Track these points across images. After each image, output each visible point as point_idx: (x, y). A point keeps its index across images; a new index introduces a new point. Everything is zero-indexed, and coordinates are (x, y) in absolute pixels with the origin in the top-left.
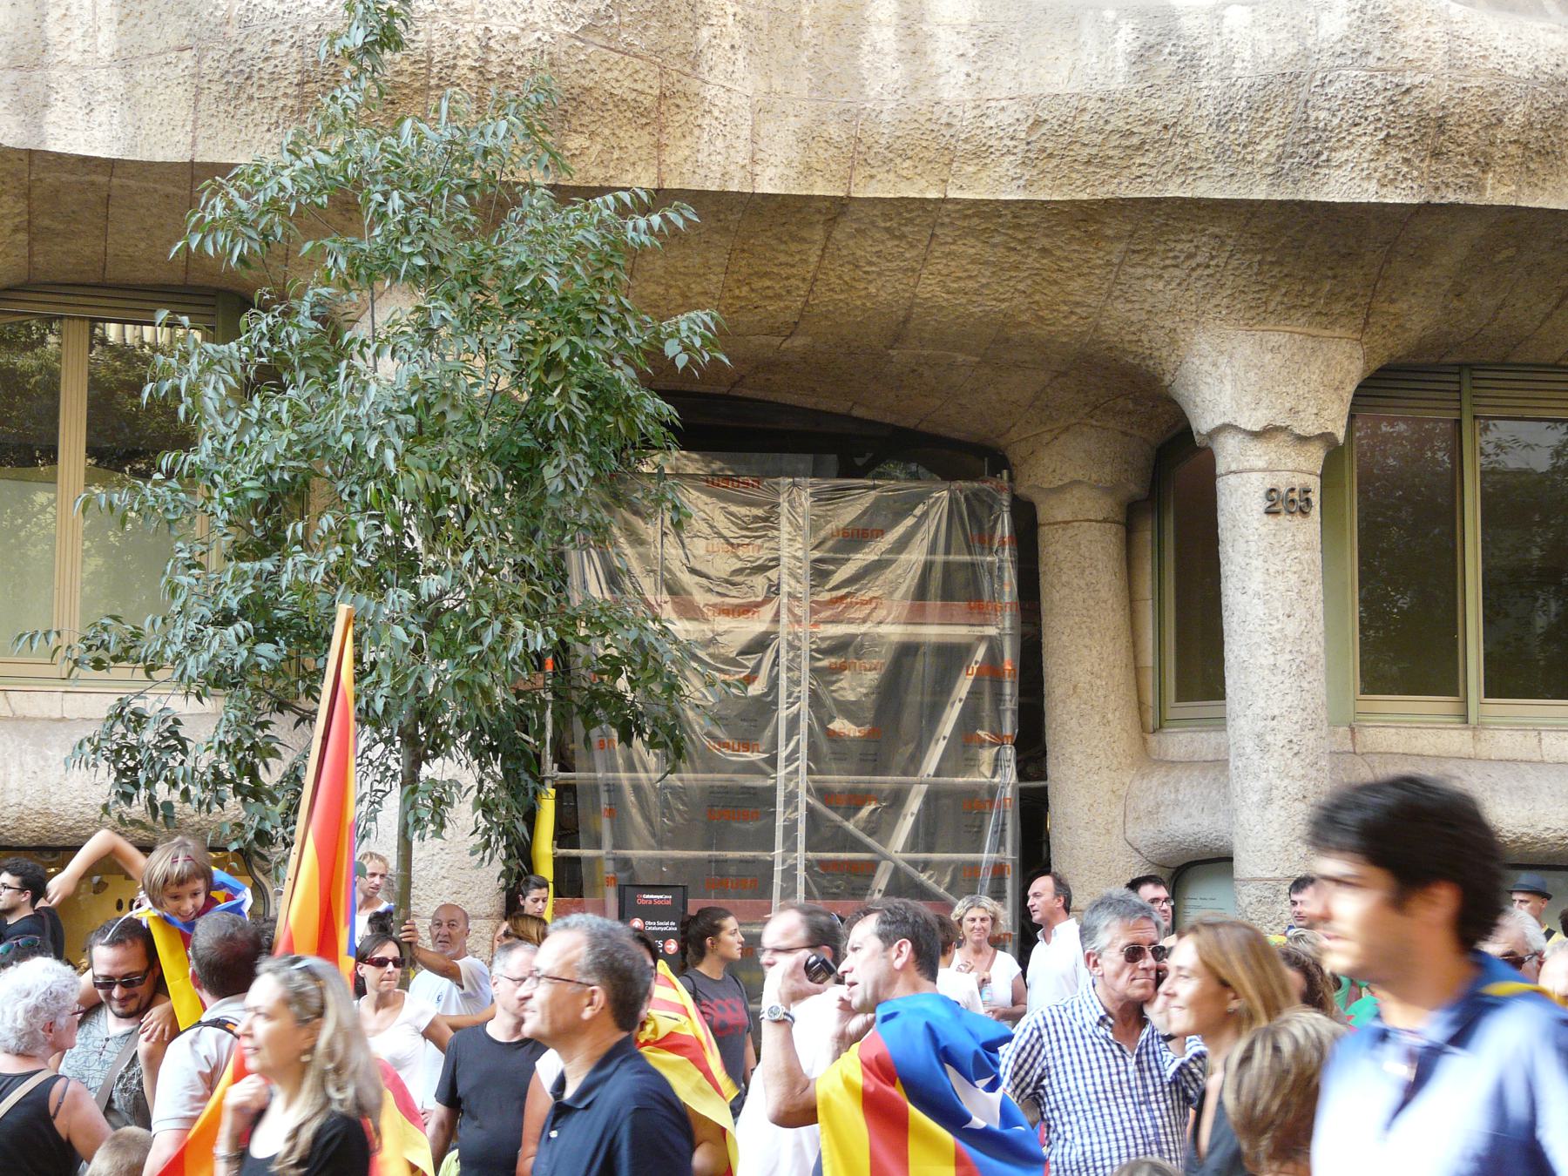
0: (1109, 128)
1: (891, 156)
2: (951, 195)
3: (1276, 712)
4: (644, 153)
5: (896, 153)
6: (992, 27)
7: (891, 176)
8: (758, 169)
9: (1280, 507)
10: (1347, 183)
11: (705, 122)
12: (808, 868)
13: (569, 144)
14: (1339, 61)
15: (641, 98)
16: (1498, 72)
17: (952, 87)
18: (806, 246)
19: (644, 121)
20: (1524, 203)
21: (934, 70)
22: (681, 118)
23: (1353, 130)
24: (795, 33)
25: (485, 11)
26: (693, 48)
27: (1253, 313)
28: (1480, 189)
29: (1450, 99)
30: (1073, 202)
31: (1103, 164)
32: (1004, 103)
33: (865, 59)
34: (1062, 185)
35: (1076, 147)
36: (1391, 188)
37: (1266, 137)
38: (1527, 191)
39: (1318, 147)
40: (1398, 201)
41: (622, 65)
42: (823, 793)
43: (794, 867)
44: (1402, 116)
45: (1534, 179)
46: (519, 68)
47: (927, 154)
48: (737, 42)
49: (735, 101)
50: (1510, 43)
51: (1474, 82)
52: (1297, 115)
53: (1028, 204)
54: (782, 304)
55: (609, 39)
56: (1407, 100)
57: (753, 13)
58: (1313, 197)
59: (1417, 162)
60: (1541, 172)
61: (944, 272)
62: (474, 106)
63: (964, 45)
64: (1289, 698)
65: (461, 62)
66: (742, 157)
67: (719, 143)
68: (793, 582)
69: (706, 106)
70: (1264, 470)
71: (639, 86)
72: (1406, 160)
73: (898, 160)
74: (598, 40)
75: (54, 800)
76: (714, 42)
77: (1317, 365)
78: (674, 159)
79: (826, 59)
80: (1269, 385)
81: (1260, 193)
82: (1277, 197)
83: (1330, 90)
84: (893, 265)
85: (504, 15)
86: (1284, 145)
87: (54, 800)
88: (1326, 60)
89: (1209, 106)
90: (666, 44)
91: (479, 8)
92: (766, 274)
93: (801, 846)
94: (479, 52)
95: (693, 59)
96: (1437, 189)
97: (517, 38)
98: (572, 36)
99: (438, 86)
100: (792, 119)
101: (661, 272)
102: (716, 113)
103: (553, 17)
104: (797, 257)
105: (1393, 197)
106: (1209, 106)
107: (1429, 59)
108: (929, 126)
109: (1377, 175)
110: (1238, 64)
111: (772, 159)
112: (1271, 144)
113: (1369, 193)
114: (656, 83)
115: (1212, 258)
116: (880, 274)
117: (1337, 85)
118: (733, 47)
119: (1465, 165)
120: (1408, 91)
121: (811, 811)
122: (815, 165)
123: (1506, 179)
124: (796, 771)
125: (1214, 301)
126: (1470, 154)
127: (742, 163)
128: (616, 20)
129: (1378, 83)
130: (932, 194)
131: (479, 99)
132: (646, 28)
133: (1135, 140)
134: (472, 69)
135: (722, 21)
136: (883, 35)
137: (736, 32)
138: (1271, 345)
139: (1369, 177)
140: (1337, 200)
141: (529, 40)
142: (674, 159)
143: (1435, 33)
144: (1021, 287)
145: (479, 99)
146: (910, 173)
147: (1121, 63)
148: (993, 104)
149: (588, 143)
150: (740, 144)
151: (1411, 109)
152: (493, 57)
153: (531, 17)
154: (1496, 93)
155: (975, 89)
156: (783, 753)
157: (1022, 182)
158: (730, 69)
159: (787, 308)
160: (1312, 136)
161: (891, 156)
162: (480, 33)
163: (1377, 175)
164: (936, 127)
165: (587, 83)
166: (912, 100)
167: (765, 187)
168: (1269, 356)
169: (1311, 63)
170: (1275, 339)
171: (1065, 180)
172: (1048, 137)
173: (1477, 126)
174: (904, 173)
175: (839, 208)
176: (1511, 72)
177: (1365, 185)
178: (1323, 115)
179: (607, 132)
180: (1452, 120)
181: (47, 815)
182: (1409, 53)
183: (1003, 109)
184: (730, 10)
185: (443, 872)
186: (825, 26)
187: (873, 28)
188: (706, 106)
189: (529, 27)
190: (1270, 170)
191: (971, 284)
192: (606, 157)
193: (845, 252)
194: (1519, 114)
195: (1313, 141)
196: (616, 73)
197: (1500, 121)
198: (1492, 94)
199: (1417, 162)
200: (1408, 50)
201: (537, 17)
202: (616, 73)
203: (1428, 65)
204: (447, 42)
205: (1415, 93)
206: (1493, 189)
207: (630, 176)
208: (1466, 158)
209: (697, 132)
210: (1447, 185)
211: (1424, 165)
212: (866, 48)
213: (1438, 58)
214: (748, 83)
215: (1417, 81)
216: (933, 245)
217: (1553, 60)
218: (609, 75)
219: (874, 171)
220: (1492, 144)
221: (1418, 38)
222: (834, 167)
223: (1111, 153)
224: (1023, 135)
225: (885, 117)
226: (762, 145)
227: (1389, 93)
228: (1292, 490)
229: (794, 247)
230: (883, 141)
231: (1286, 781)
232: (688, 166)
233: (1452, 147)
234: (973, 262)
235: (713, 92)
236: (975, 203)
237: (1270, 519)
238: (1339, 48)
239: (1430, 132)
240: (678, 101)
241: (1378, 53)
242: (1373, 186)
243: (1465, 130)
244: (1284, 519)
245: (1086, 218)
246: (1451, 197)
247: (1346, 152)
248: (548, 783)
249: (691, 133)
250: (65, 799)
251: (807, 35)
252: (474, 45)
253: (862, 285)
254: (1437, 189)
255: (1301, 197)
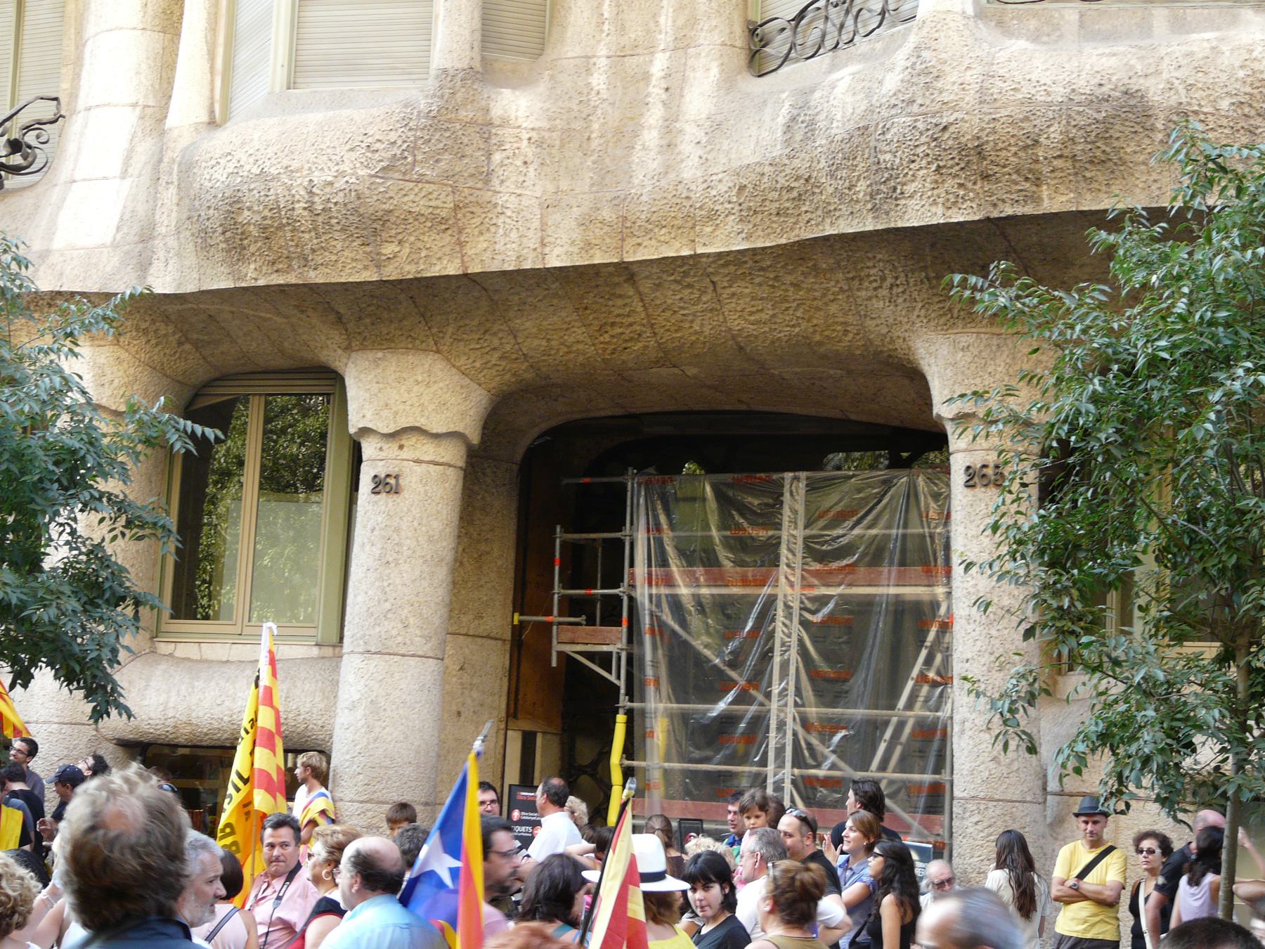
0: (779, 186)
1: (650, 227)
2: (699, 251)
3: (969, 656)
4: (447, 249)
5: (655, 224)
6: (719, 117)
7: (653, 242)
8: (547, 250)
9: (976, 479)
10: (920, 212)
11: (500, 221)
12: (794, 782)
13: (384, 251)
14: (893, 112)
15: (438, 211)
16: (1030, 100)
17: (690, 171)
18: (628, 301)
19: (444, 227)
20: (1085, 208)
21: (680, 156)
22: (477, 221)
23: (912, 166)
24: (584, 145)
25: (310, 169)
26: (485, 169)
27: (942, 321)
28: (1037, 200)
29: (982, 130)
30: (778, 246)
31: (787, 215)
32: (720, 176)
33: (637, 155)
34: (769, 235)
35: (767, 203)
36: (955, 210)
37: (858, 180)
38: (1088, 196)
39: (892, 183)
40: (961, 219)
41: (417, 190)
42: (805, 723)
43: (782, 781)
44: (945, 150)
45: (1095, 185)
46: (336, 204)
47: (676, 222)
48: (530, 158)
49: (525, 202)
50: (1048, 73)
51: (1004, 113)
52: (871, 160)
53: (754, 251)
54: (640, 345)
55: (404, 174)
56: (946, 135)
57: (547, 135)
58: (900, 224)
59: (970, 185)
60: (1101, 178)
61: (739, 309)
62: (313, 234)
63: (700, 135)
64: (979, 643)
65: (297, 206)
66: (533, 242)
67: (514, 235)
68: (790, 556)
69: (499, 209)
70: (965, 451)
71: (431, 203)
72: (961, 185)
73: (656, 230)
74: (397, 175)
75: (194, 715)
76: (506, 162)
77: (1003, 358)
78: (473, 251)
79: (607, 160)
80: (960, 378)
81: (869, 225)
82: (880, 227)
83: (889, 136)
84: (699, 308)
85: (322, 169)
86: (870, 185)
87: (194, 715)
88: (885, 113)
89: (823, 161)
90: (457, 169)
91: (306, 167)
92: (613, 324)
93: (788, 764)
94: (306, 197)
95: (487, 178)
96: (995, 205)
97: (331, 184)
98: (373, 176)
99: (289, 224)
100: (575, 209)
101: (534, 330)
102: (509, 213)
103: (358, 165)
104: (627, 309)
105: (957, 217)
106: (823, 161)
107: (963, 99)
108: (675, 200)
109: (941, 200)
110: (835, 125)
111: (558, 241)
112: (862, 186)
113: (936, 216)
114: (450, 198)
115: (897, 278)
116: (694, 315)
117: (893, 131)
118: (525, 163)
119: (1016, 183)
120: (945, 128)
121: (795, 734)
122: (594, 241)
123: (1062, 188)
124: (786, 705)
125: (916, 313)
126: (1018, 172)
127: (532, 246)
128: (410, 159)
129: (921, 125)
130: (686, 252)
131: (315, 229)
132: (437, 161)
133: (795, 194)
134: (305, 209)
135: (516, 145)
136: (651, 137)
137: (528, 151)
138: (961, 345)
139: (935, 203)
140: (916, 225)
141: (340, 184)
142: (473, 251)
143: (971, 77)
144: (799, 314)
145: (315, 229)
146: (667, 238)
147: (779, 133)
148: (714, 177)
149: (397, 249)
150: (530, 234)
151: (950, 142)
152: (316, 199)
153: (342, 168)
154: (1026, 119)
155: (704, 168)
156: (776, 689)
157: (744, 235)
158: (521, 179)
159: (646, 347)
160: (886, 175)
161: (650, 227)
162: (306, 184)
163: (941, 200)
164: (679, 201)
165: (386, 207)
166: (663, 183)
167: (554, 262)
168: (961, 354)
169: (875, 117)
170: (964, 340)
171: (769, 230)
172: (754, 199)
173: (1014, 149)
174: (662, 239)
175: (627, 271)
176: (1042, 99)
177: (934, 209)
178: (888, 157)
179: (412, 239)
180: (988, 147)
181: (190, 724)
182: (946, 97)
183: (720, 181)
184: (525, 136)
185: (359, 770)
186: (610, 135)
187: (646, 132)
188: (499, 209)
189: (341, 174)
190: (869, 206)
191: (764, 316)
192: (413, 256)
193: (658, 302)
194: (1055, 132)
195: (888, 179)
196: (411, 197)
197: (1037, 141)
198: (1022, 121)
199: (970, 185)
200: (944, 94)
201: (346, 167)
202: (411, 197)
203: (962, 104)
204: (286, 193)
205: (952, 129)
206: (1051, 199)
207: (438, 268)
208: (1014, 177)
209: (493, 229)
210: (1003, 201)
211: (976, 187)
212: (638, 147)
213: (970, 98)
214: (537, 187)
215: (951, 119)
216: (719, 290)
217: (1097, 81)
218: (406, 199)
219: (639, 240)
220: (1037, 161)
221: (954, 83)
222: (608, 240)
223: (787, 205)
224: (735, 199)
225: (644, 198)
226: (550, 232)
227: (930, 133)
228: (984, 466)
229: (620, 302)
230: (643, 217)
231: (974, 716)
232: (488, 254)
233: (997, 169)
234: (753, 299)
235: (504, 199)
236: (719, 255)
237: (969, 492)
238: (893, 101)
239: (973, 159)
240: (473, 209)
241: (919, 101)
242: (939, 210)
243: (1004, 153)
244: (979, 491)
245: (802, 253)
246: (1009, 211)
247: (914, 185)
248: (621, 711)
249: (488, 229)
250: (201, 714)
251: (595, 144)
252: (303, 192)
253: (687, 325)
254: (995, 205)
255: (892, 225)
